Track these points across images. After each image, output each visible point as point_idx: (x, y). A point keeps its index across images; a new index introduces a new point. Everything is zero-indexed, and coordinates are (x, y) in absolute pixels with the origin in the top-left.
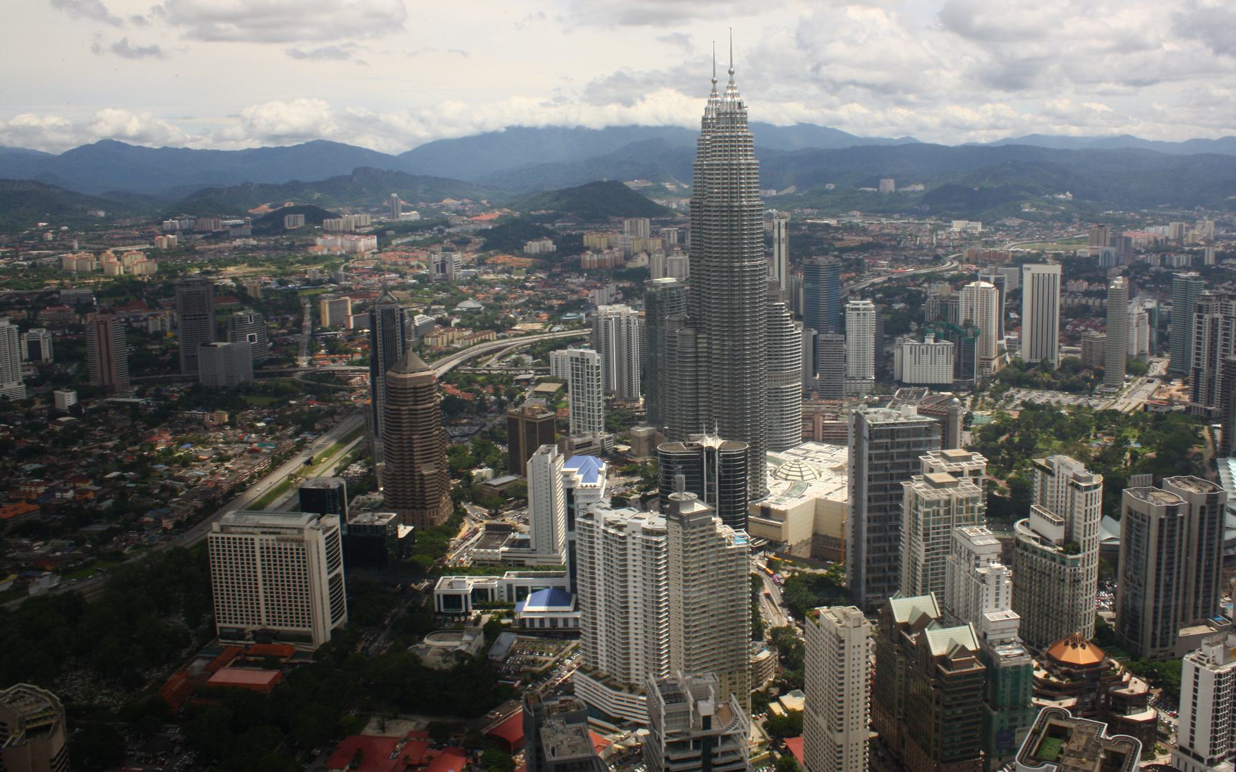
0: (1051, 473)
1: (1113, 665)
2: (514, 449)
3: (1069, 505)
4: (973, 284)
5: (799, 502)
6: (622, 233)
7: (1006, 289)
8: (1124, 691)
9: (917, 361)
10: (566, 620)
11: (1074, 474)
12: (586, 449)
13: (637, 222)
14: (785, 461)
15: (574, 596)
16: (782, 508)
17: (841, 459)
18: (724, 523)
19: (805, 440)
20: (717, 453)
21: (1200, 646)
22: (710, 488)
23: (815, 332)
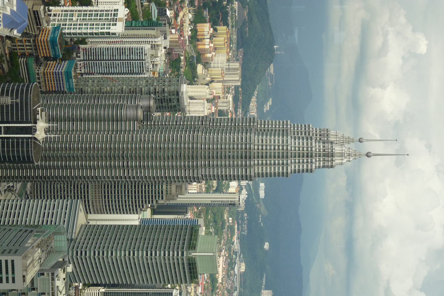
6: (228, 60)
13: (237, 74)
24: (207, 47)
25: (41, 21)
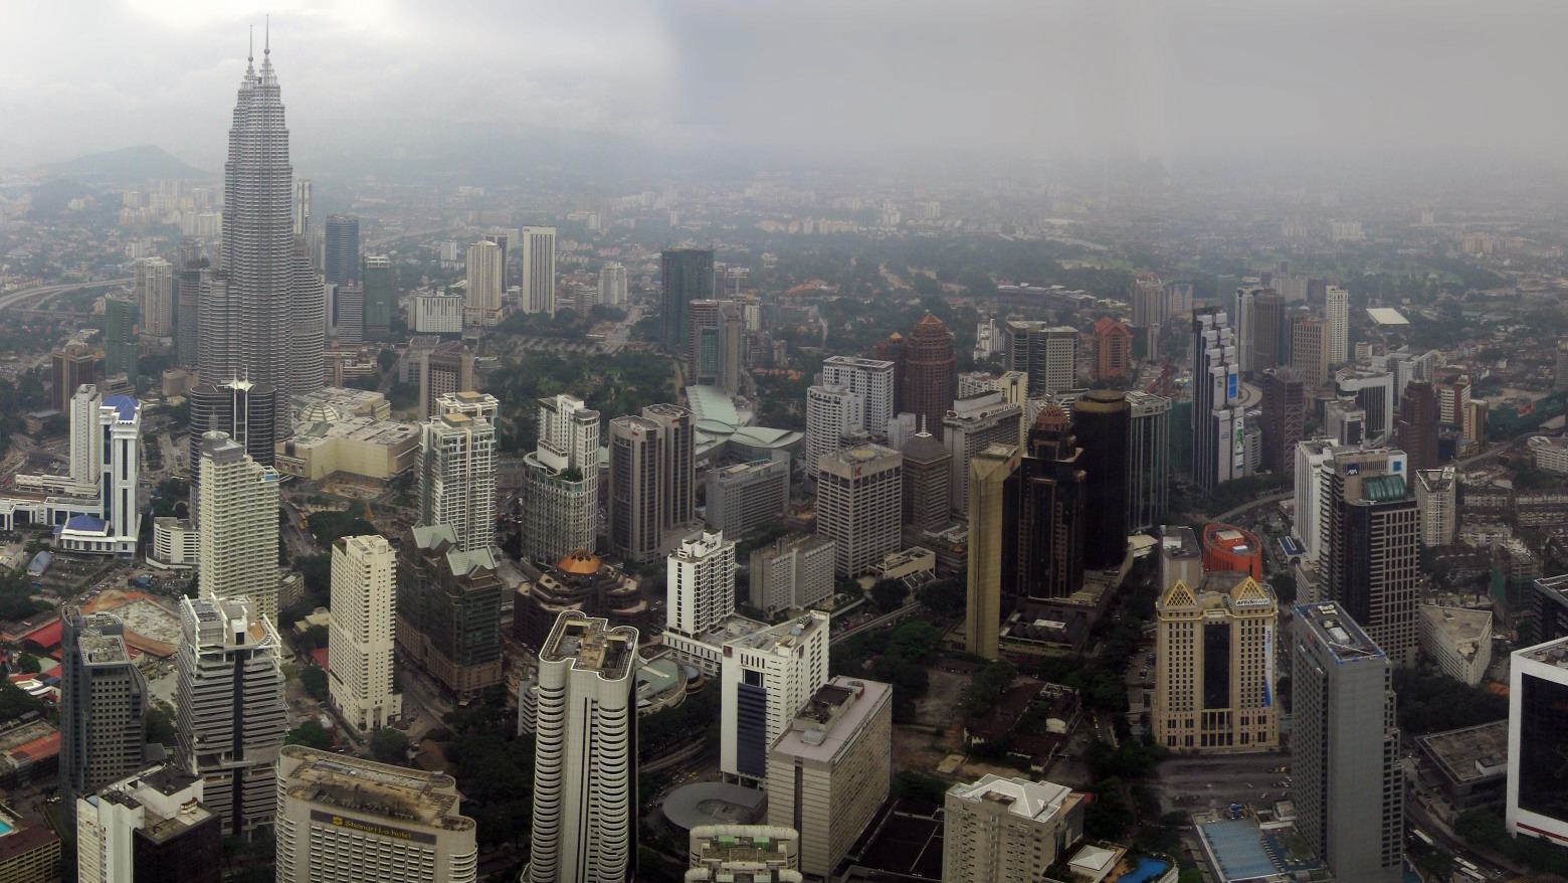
0: (552, 409)
1: (609, 570)
2: (58, 389)
3: (571, 438)
7: (509, 248)
8: (620, 590)
9: (429, 312)
10: (99, 544)
11: (576, 411)
14: (308, 404)
15: (108, 522)
16: (306, 446)
18: (254, 461)
19: (326, 385)
21: (681, 544)
22: (241, 427)
23: (336, 285)
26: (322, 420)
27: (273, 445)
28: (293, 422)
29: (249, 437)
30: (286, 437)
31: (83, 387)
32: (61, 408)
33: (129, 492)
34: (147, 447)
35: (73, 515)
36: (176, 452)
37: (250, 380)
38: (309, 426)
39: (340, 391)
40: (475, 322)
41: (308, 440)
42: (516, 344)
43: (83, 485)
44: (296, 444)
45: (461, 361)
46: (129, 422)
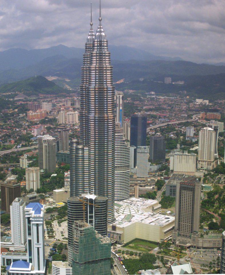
4: (205, 128)
5: (129, 224)
12: (34, 199)
14: (122, 205)
15: (31, 264)
16: (121, 226)
17: (147, 205)
20: (94, 202)
23: (135, 148)
24: (39, 113)
25: (34, 196)
26: (129, 213)
27: (106, 225)
28: (115, 214)
29: (95, 222)
30: (112, 221)
31: (17, 199)
32: (6, 210)
33: (40, 249)
34: (47, 227)
35: (15, 261)
36: (61, 229)
37: (95, 194)
38: (123, 216)
39: (137, 199)
40: (202, 167)
41: (122, 223)
42: (220, 178)
43: (18, 246)
44: (117, 226)
45: (195, 186)
46: (39, 215)
